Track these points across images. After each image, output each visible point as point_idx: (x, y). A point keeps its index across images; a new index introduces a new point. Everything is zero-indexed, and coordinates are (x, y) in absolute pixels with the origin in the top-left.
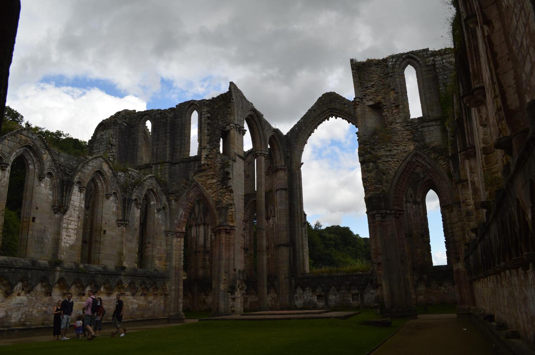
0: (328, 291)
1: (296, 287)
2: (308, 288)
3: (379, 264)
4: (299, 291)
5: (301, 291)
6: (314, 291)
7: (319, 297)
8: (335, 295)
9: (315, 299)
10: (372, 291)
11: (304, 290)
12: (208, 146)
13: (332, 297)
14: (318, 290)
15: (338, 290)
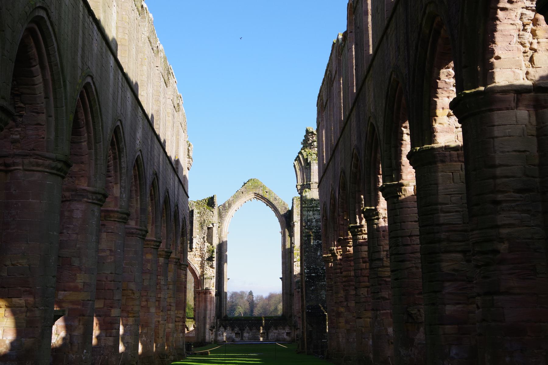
0: (244, 330)
1: (220, 327)
2: (229, 328)
3: (299, 317)
4: (222, 329)
5: (223, 330)
6: (233, 330)
7: (236, 334)
8: (249, 333)
9: (233, 335)
10: (275, 331)
11: (225, 329)
12: (198, 236)
13: (246, 335)
14: (236, 329)
15: (251, 330)
